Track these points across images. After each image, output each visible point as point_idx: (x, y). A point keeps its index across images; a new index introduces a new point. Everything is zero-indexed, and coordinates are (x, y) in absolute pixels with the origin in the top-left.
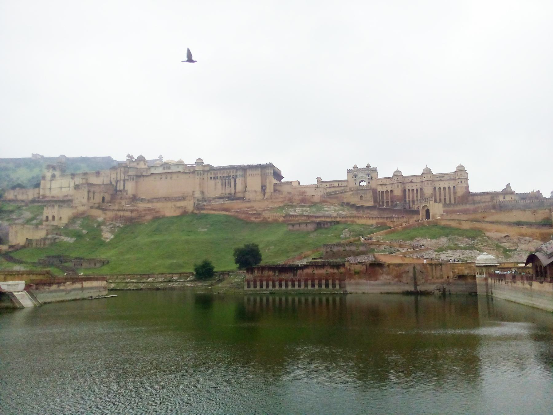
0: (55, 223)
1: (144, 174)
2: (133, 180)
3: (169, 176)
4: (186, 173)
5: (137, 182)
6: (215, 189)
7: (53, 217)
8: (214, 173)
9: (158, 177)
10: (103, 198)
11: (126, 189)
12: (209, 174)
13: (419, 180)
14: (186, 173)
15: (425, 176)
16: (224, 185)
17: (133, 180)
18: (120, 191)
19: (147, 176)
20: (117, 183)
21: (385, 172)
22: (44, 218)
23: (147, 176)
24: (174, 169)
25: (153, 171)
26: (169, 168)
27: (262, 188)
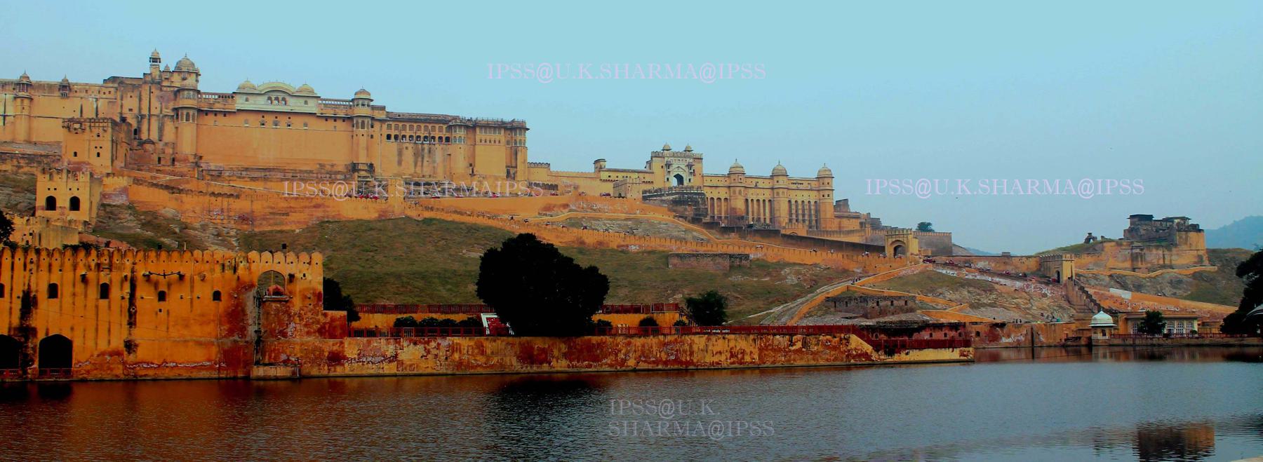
3: (283, 120)
4: (327, 118)
6: (400, 163)
8: (397, 128)
9: (254, 120)
12: (385, 126)
13: (767, 184)
14: (327, 118)
15: (781, 179)
16: (418, 155)
19: (225, 113)
20: (139, 122)
21: (716, 165)
22: (41, 202)
23: (225, 113)
24: (295, 105)
27: (508, 172)
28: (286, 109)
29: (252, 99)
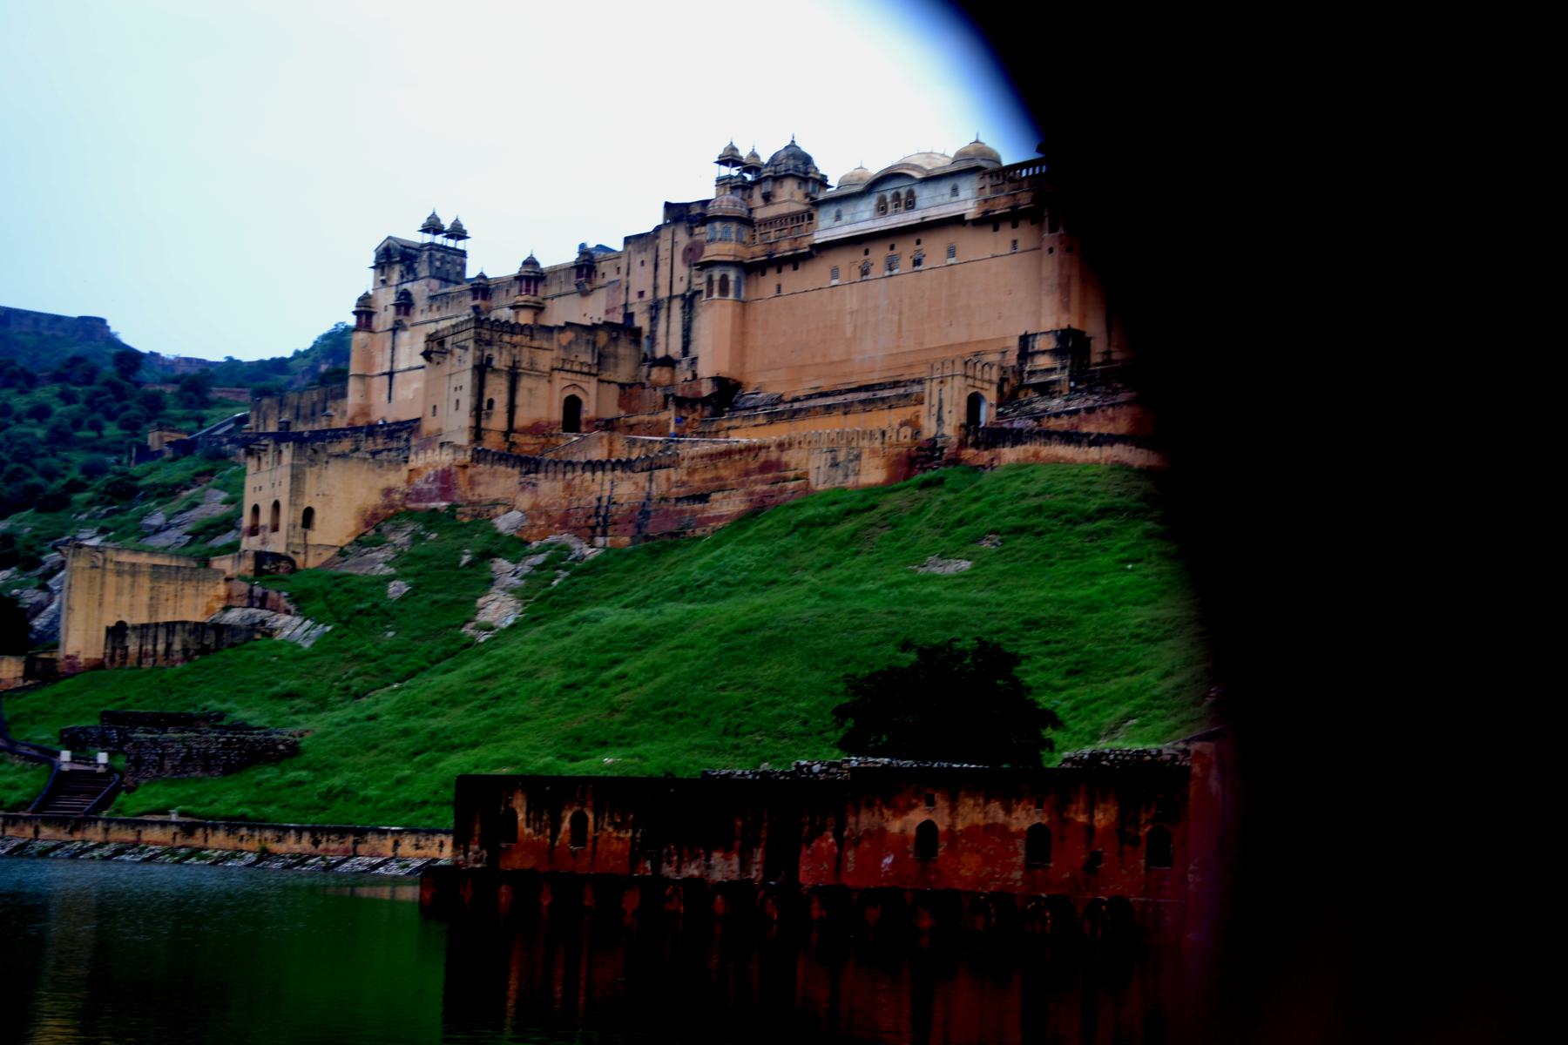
0: (277, 544)
1: (785, 248)
2: (724, 290)
3: (906, 249)
5: (743, 304)
7: (276, 505)
9: (847, 261)
10: (572, 406)
11: (693, 349)
17: (724, 290)
18: (668, 362)
20: (654, 320)
22: (246, 521)
23: (796, 260)
24: (933, 204)
25: (827, 228)
26: (910, 204)
28: (912, 218)
29: (848, 210)
